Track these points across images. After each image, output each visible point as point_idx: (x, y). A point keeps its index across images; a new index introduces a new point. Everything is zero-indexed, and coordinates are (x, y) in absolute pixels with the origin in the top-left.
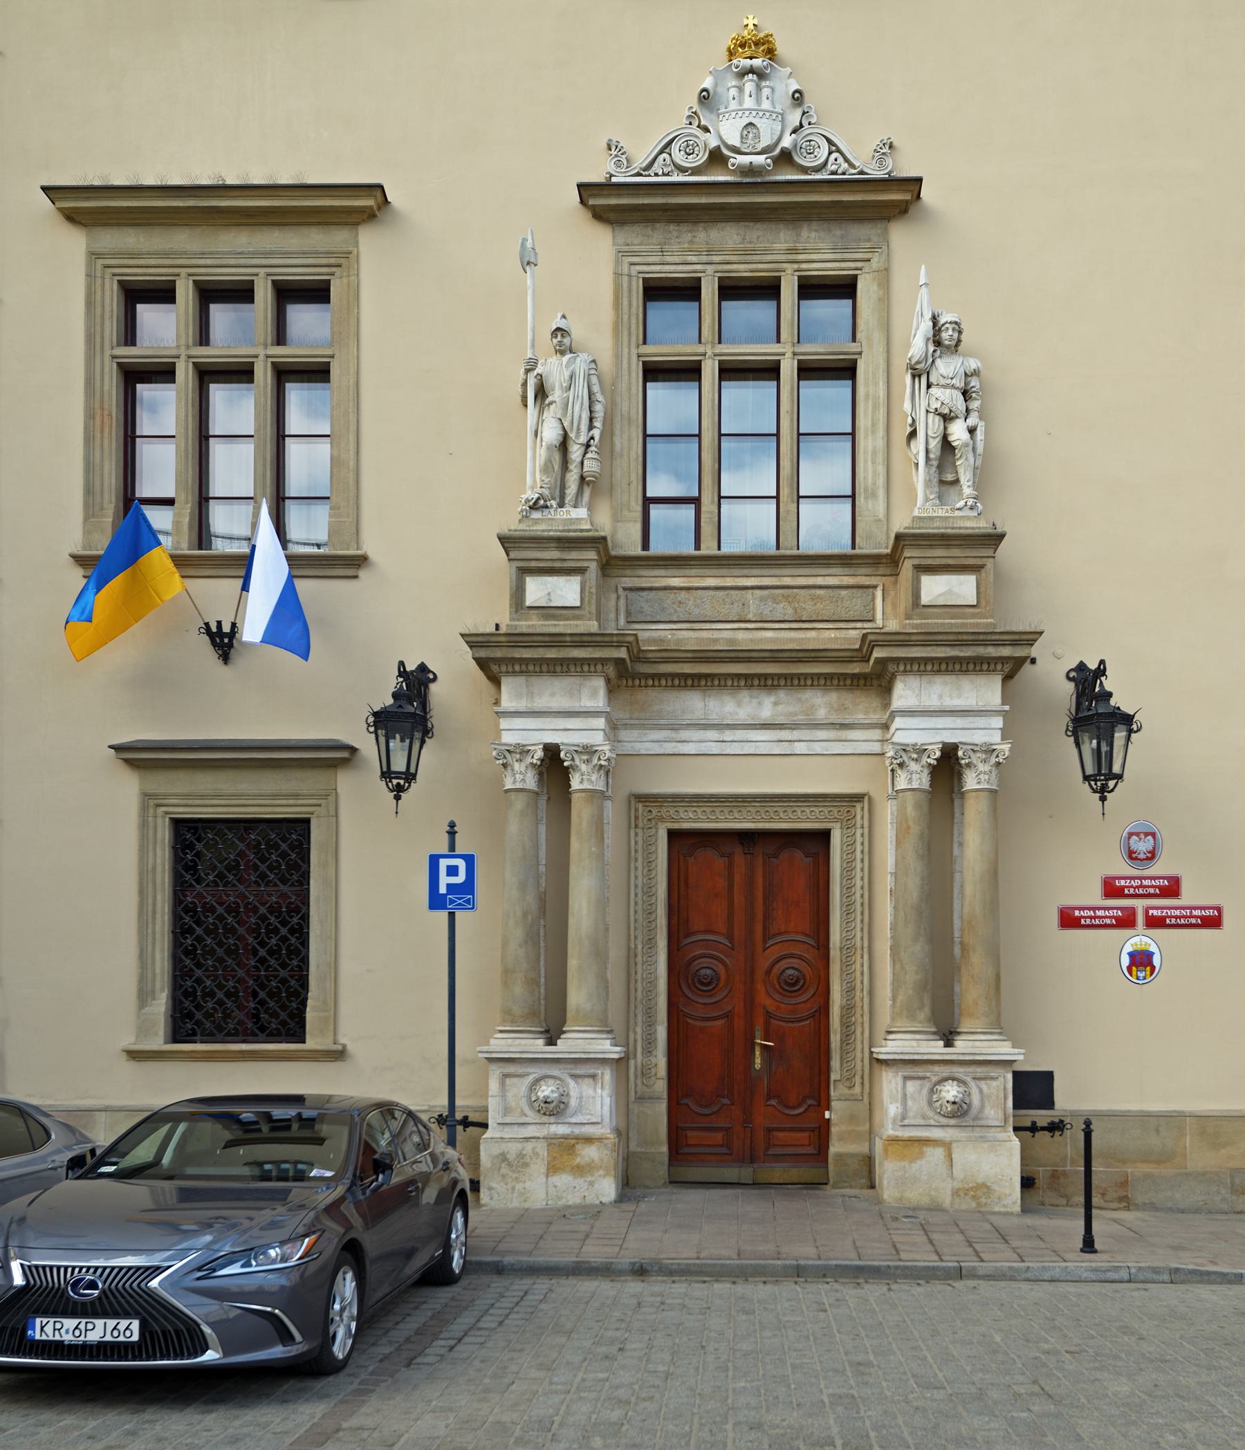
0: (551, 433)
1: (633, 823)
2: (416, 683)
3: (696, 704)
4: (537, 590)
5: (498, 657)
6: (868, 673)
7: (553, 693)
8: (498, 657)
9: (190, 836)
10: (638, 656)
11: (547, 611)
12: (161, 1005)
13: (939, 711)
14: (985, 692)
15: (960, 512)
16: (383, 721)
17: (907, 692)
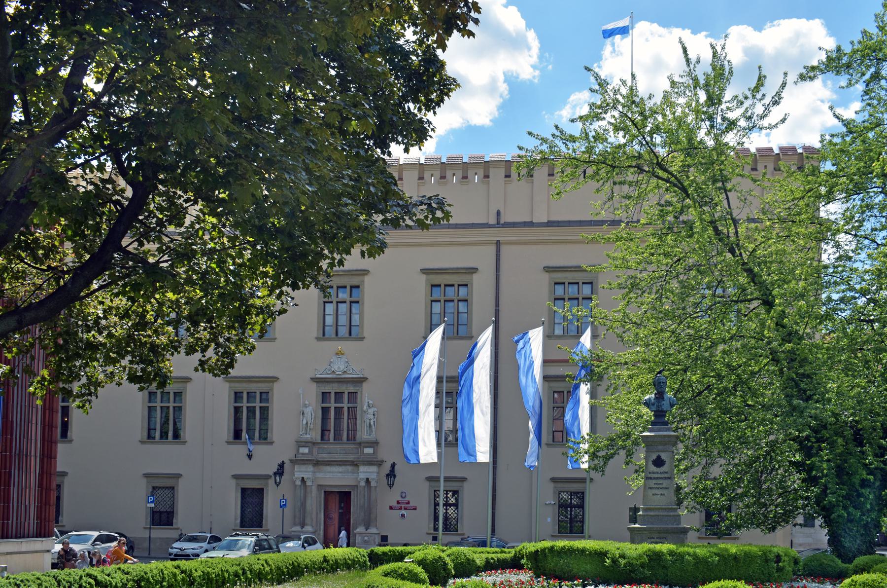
0: (305, 422)
1: (318, 490)
2: (282, 466)
3: (328, 468)
4: (302, 450)
5: (294, 462)
6: (355, 464)
7: (303, 468)
8: (294, 462)
9: (244, 491)
10: (318, 461)
11: (303, 454)
12: (239, 521)
13: (366, 472)
14: (374, 469)
15: (372, 437)
16: (275, 474)
17: (362, 468)
